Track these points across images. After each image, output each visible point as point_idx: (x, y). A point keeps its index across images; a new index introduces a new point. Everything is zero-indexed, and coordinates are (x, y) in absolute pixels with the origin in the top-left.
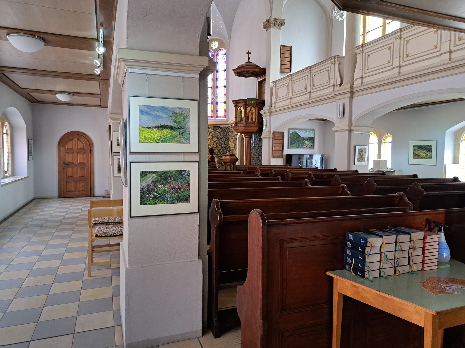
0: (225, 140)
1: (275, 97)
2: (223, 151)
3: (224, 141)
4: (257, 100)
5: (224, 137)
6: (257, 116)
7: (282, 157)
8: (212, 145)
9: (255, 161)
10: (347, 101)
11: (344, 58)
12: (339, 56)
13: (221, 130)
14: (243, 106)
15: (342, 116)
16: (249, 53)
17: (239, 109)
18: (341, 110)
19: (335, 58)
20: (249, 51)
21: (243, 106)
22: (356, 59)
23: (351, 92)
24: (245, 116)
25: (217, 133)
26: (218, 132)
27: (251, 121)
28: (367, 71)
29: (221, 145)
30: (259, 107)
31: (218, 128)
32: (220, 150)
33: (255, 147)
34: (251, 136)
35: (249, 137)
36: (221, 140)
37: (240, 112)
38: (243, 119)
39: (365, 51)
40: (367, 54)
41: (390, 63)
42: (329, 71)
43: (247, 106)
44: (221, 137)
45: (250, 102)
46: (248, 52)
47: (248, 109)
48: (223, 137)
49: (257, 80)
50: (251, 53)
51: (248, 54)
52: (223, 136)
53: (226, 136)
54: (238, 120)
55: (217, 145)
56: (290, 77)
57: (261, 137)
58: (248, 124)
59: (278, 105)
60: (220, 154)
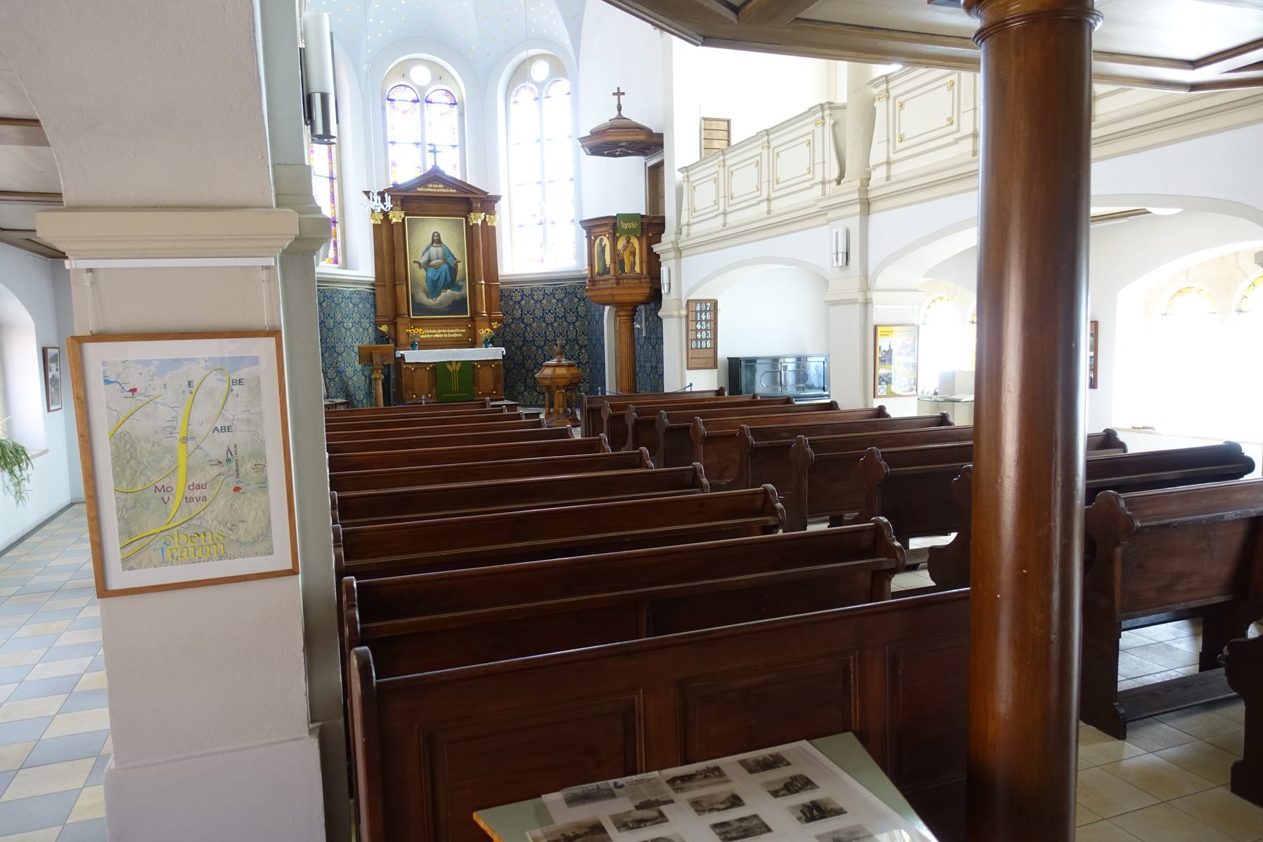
1: (689, 209)
2: (572, 348)
3: (573, 323)
4: (642, 217)
5: (573, 313)
6: (645, 258)
7: (715, 366)
9: (648, 375)
10: (854, 224)
11: (846, 108)
12: (832, 103)
14: (607, 236)
15: (845, 264)
16: (619, 94)
17: (598, 241)
18: (842, 248)
19: (823, 110)
20: (618, 89)
21: (607, 236)
22: (873, 112)
23: (863, 201)
24: (613, 261)
25: (554, 301)
26: (558, 300)
27: (631, 272)
28: (899, 146)
29: (567, 332)
30: (651, 235)
33: (648, 340)
34: (634, 310)
35: (627, 316)
37: (600, 250)
38: (609, 268)
39: (893, 93)
40: (898, 100)
41: (952, 124)
42: (811, 143)
43: (618, 235)
45: (625, 226)
46: (616, 91)
47: (621, 244)
49: (645, 164)
50: (623, 94)
51: (617, 96)
52: (571, 310)
53: (577, 308)
54: (596, 271)
55: (555, 333)
56: (721, 158)
57: (660, 314)
58: (621, 282)
59: (694, 229)
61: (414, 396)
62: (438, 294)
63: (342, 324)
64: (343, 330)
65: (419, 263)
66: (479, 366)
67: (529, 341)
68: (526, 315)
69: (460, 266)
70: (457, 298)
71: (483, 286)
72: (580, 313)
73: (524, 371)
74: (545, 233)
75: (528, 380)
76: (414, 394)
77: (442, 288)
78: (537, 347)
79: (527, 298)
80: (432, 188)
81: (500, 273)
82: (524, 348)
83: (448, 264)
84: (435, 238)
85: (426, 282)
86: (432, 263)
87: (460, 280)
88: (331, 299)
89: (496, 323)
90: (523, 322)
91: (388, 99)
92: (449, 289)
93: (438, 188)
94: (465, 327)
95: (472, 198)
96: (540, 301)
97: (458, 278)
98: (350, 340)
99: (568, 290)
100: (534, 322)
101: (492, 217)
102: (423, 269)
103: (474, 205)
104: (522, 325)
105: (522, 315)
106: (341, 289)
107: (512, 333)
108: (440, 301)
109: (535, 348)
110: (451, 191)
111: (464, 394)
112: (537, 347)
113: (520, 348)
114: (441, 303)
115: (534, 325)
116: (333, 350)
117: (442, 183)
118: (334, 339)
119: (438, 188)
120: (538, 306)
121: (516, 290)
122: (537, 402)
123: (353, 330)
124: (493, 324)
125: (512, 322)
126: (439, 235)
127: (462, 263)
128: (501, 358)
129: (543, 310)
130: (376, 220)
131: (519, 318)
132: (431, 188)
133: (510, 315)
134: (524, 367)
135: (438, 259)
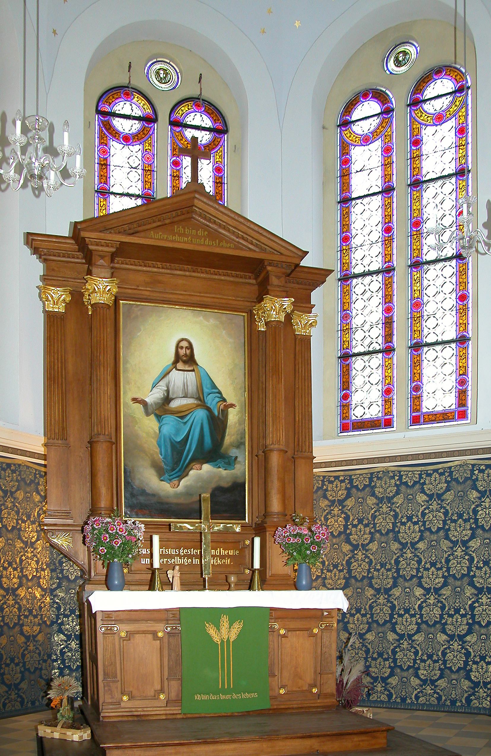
0: (473, 537)
2: (457, 594)
3: (465, 543)
5: (465, 521)
13: (446, 482)
26: (431, 497)
31: (429, 475)
32: (437, 591)
36: (447, 537)
44: (444, 522)
48: (455, 521)
52: (460, 516)
55: (419, 562)
60: (437, 612)
67: (359, 577)
72: (481, 522)
77: (192, 460)
78: (378, 591)
79: (360, 494)
83: (208, 409)
85: (160, 446)
96: (390, 499)
99: (456, 475)
100: (372, 540)
102: (152, 417)
105: (346, 527)
109: (372, 592)
112: (378, 591)
129: (396, 516)
135: (186, 396)
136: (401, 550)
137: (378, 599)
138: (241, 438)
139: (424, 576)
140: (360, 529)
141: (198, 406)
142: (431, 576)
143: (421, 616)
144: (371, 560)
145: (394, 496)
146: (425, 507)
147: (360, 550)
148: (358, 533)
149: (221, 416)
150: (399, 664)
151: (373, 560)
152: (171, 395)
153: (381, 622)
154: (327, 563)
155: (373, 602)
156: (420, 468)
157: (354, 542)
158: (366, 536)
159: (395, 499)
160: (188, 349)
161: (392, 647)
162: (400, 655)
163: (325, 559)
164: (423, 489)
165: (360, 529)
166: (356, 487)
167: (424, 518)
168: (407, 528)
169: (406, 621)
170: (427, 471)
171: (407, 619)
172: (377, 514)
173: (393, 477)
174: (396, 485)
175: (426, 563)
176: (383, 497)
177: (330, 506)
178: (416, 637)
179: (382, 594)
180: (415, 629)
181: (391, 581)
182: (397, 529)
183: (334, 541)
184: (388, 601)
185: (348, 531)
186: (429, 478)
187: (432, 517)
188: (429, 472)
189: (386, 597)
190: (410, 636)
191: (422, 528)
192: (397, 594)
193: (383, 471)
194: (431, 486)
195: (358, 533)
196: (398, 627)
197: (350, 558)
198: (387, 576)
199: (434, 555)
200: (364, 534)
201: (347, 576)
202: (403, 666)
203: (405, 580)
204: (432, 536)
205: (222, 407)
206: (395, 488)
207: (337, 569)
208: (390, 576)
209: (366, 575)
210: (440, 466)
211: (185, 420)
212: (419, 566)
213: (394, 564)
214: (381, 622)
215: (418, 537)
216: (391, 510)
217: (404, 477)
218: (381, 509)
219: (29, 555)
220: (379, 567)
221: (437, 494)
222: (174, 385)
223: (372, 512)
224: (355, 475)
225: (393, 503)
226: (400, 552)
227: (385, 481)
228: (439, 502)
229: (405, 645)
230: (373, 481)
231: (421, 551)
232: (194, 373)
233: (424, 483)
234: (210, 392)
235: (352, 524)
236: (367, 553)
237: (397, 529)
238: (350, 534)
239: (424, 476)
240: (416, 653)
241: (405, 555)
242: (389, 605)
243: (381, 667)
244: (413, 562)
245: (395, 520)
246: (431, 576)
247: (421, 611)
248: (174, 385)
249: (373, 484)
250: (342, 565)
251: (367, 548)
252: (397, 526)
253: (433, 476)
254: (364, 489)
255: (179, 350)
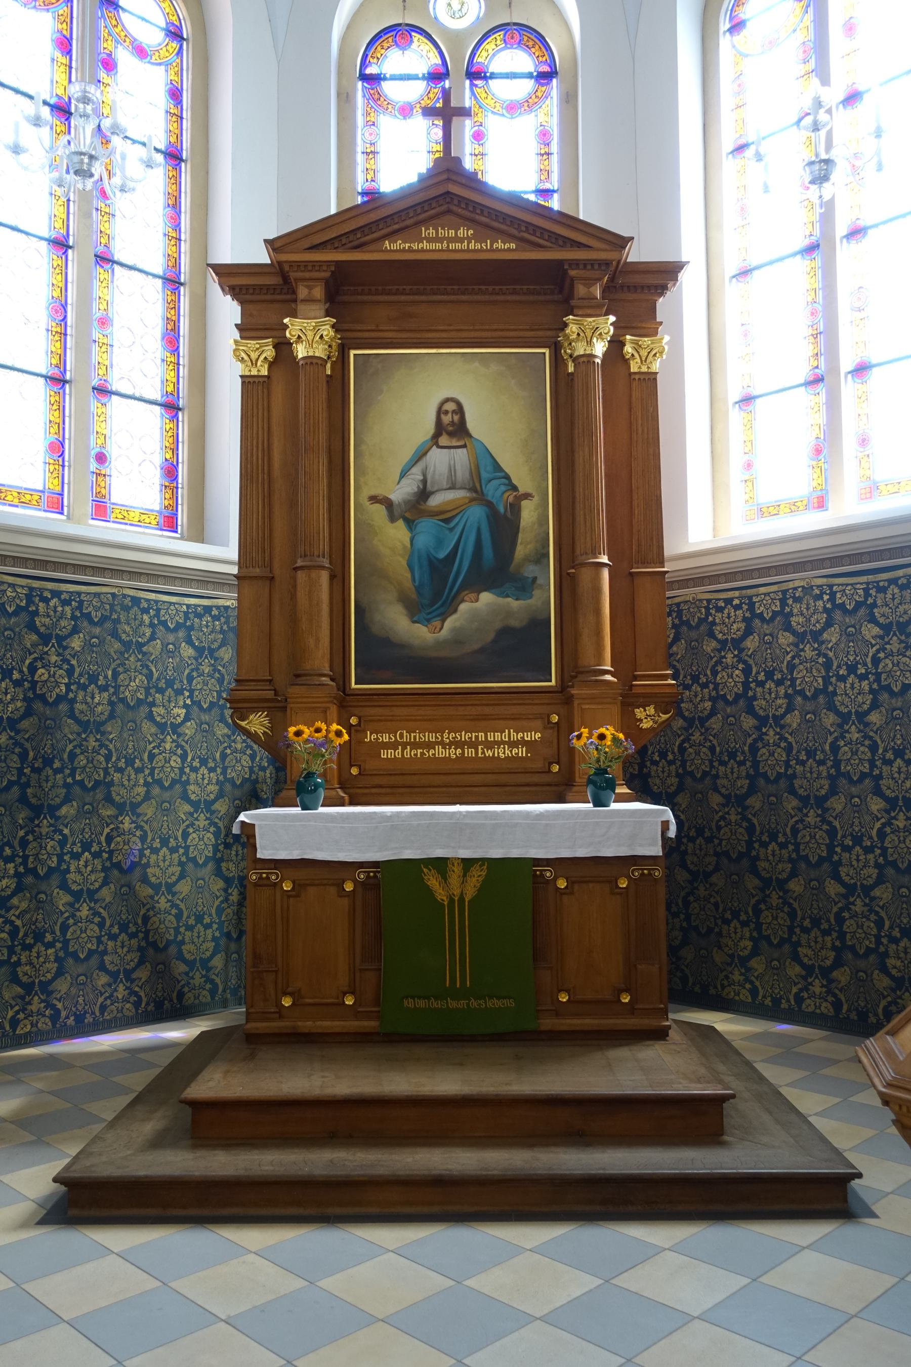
8: (820, 756)
25: (870, 631)
31: (882, 590)
55: (874, 748)
61: (287, 1002)
62: (450, 608)
63: (144, 710)
64: (148, 728)
65: (387, 503)
66: (562, 884)
67: (772, 775)
68: (761, 684)
69: (528, 513)
70: (515, 623)
71: (606, 573)
73: (752, 882)
74: (833, 406)
75: (766, 917)
76: (285, 994)
78: (805, 800)
80: (437, 239)
81: (671, 547)
82: (754, 802)
83: (490, 505)
84: (446, 419)
86: (435, 501)
87: (527, 559)
88: (108, 625)
89: (651, 710)
90: (751, 711)
91: (364, 77)
92: (485, 590)
93: (457, 239)
94: (538, 723)
95: (575, 264)
96: (816, 636)
97: (521, 551)
98: (175, 762)
100: (790, 709)
101: (646, 341)
102: (401, 523)
103: (581, 290)
104: (748, 722)
105: (746, 685)
106: (153, 596)
107: (712, 749)
108: (454, 630)
109: (795, 803)
110: (499, 245)
111: (496, 1003)
112: (805, 800)
113: (741, 800)
114: (457, 640)
115: (793, 720)
116: (100, 795)
117: (470, 222)
118: (108, 758)
119: (457, 239)
120: (809, 652)
121: (728, 601)
122: (799, 1000)
123: (189, 729)
124: (639, 713)
125: (713, 713)
126: (460, 410)
127: (536, 499)
128: (656, 850)
129: (828, 665)
130: (254, 363)
131: (738, 697)
132: (430, 240)
133: (705, 686)
134: (754, 871)
135: (453, 487)
136: (840, 726)
137: (806, 815)
138: (543, 548)
139: (885, 774)
140: (770, 689)
141: (471, 500)
142: (896, 775)
143: (884, 850)
144: (790, 744)
145: (823, 630)
146: (878, 647)
147: (771, 726)
148: (767, 696)
149: (509, 514)
150: (850, 943)
151: (794, 744)
152: (429, 487)
153: (814, 859)
154: (718, 749)
155: (797, 822)
156: (864, 579)
157: (762, 713)
158: (779, 702)
159: (825, 635)
160: (456, 413)
161: (835, 909)
162: (849, 925)
163: (715, 742)
164: (872, 614)
165: (770, 689)
166: (761, 616)
167: (877, 668)
168: (848, 685)
169: (858, 860)
170: (878, 582)
171: (858, 856)
172: (796, 661)
173: (819, 597)
174: (825, 610)
175: (885, 750)
176: (805, 631)
177: (719, 651)
178: (877, 892)
179: (812, 808)
180: (874, 876)
181: (826, 783)
182: (831, 689)
183: (729, 710)
184: (824, 820)
185: (750, 694)
186: (882, 595)
187: (890, 665)
188: (881, 584)
189: (820, 812)
190: (867, 890)
191: (875, 686)
192: (839, 807)
193: (803, 587)
194: (886, 610)
195: (767, 696)
196: (843, 871)
197: (755, 741)
198: (819, 774)
199: (898, 736)
200: (776, 698)
201: (752, 772)
202: (858, 947)
203: (851, 781)
204: (894, 701)
205: (511, 499)
206: (825, 615)
207: (735, 761)
208: (824, 774)
209: (782, 771)
210: (900, 573)
211: (452, 525)
212: (873, 755)
213: (829, 752)
214: (814, 859)
215: (868, 702)
216: (819, 655)
217: (838, 595)
218: (802, 653)
219: (239, 746)
220: (805, 758)
221: (898, 623)
222: (434, 471)
223: (788, 658)
224: (757, 595)
225: (823, 642)
226: (839, 730)
227: (808, 605)
228: (903, 638)
229: (859, 907)
230: (788, 605)
231: (875, 729)
232: (464, 450)
233: (874, 605)
234: (491, 476)
235: (756, 681)
236: (783, 732)
237: (831, 689)
238: (754, 698)
239: (873, 592)
240: (880, 924)
241: (847, 735)
242: (825, 827)
243: (819, 946)
244: (862, 749)
245: (827, 672)
246: (896, 775)
247: (883, 842)
248: (434, 471)
249: (787, 609)
250: (743, 752)
251: (782, 722)
252: (831, 683)
253: (890, 592)
254: (772, 619)
255: (443, 416)
